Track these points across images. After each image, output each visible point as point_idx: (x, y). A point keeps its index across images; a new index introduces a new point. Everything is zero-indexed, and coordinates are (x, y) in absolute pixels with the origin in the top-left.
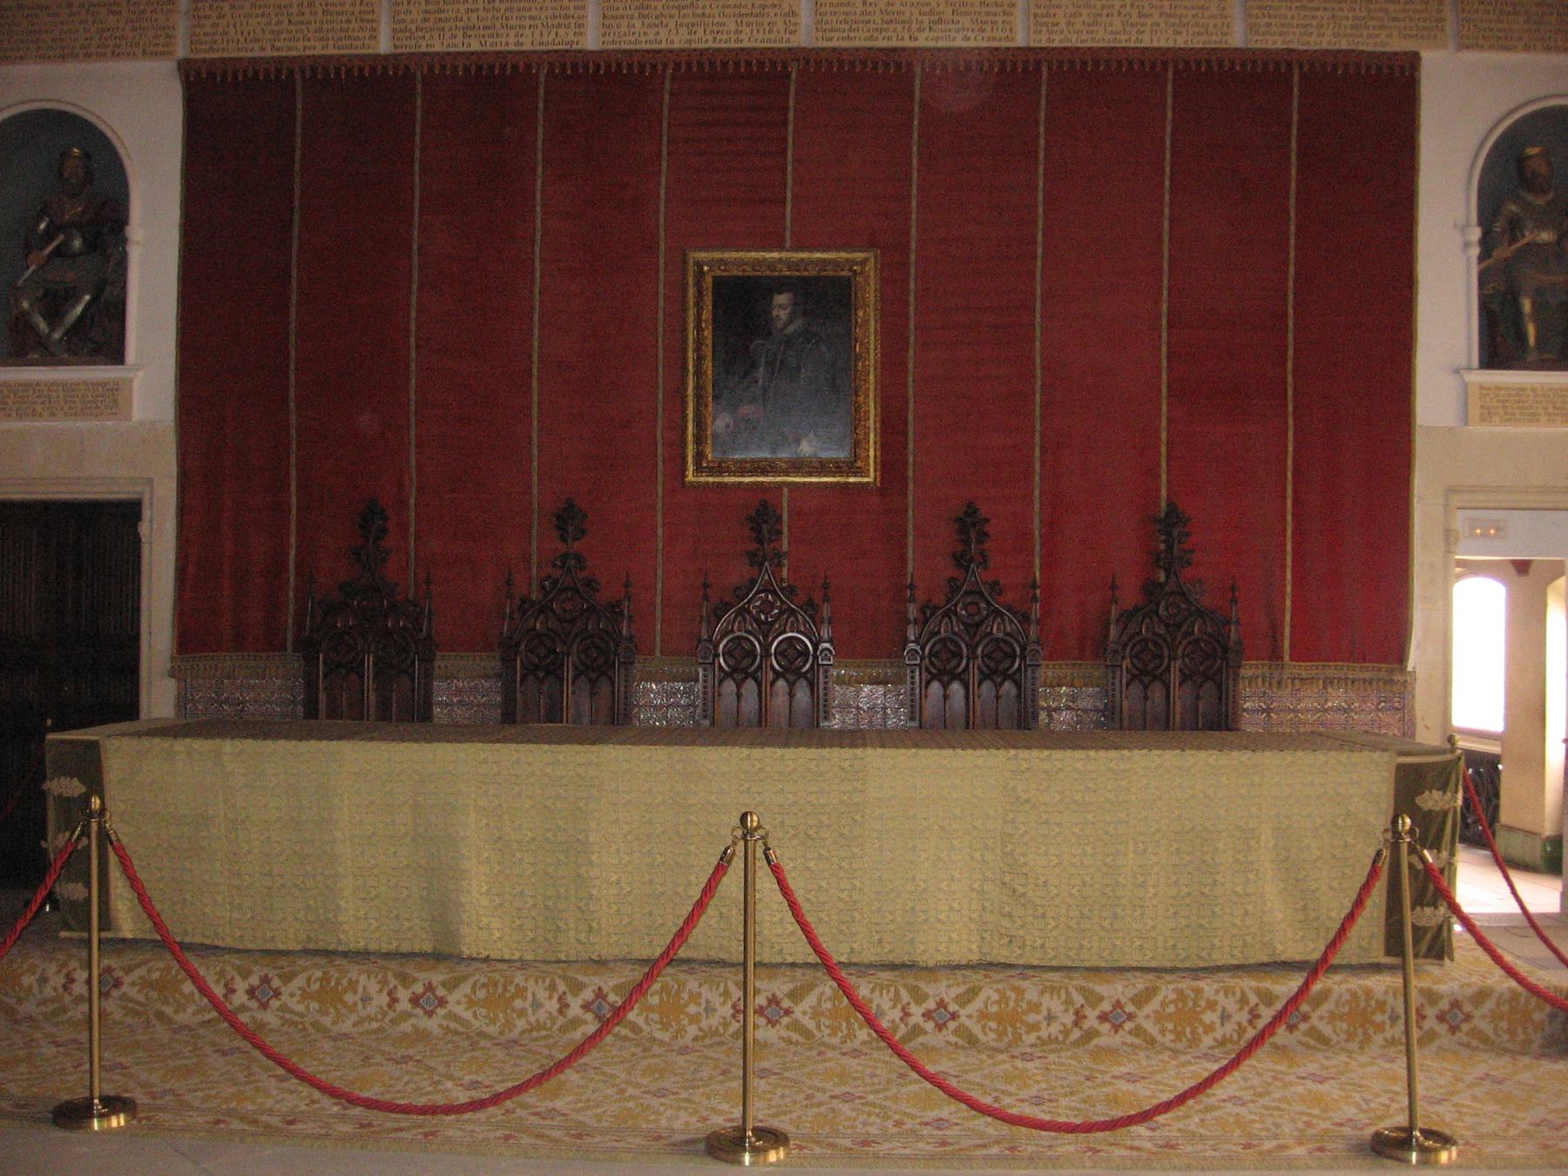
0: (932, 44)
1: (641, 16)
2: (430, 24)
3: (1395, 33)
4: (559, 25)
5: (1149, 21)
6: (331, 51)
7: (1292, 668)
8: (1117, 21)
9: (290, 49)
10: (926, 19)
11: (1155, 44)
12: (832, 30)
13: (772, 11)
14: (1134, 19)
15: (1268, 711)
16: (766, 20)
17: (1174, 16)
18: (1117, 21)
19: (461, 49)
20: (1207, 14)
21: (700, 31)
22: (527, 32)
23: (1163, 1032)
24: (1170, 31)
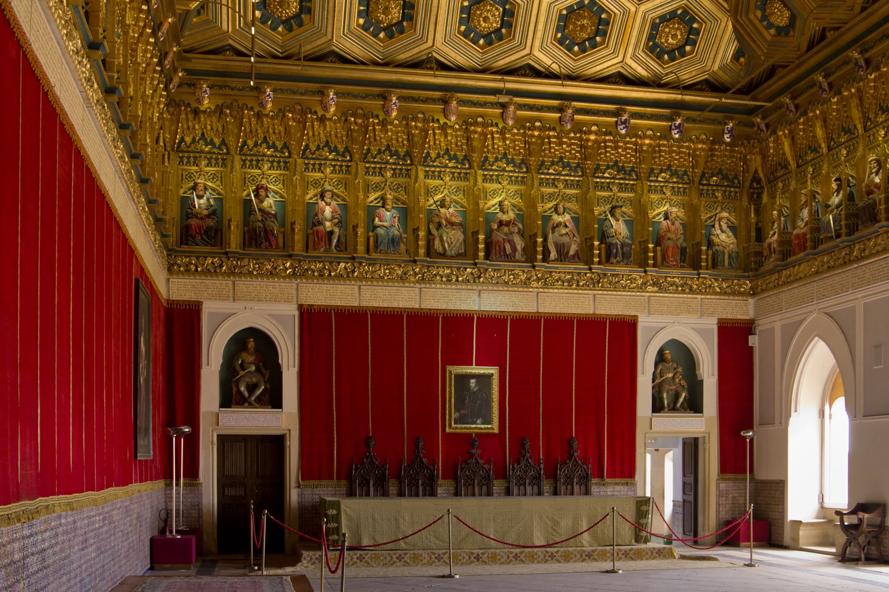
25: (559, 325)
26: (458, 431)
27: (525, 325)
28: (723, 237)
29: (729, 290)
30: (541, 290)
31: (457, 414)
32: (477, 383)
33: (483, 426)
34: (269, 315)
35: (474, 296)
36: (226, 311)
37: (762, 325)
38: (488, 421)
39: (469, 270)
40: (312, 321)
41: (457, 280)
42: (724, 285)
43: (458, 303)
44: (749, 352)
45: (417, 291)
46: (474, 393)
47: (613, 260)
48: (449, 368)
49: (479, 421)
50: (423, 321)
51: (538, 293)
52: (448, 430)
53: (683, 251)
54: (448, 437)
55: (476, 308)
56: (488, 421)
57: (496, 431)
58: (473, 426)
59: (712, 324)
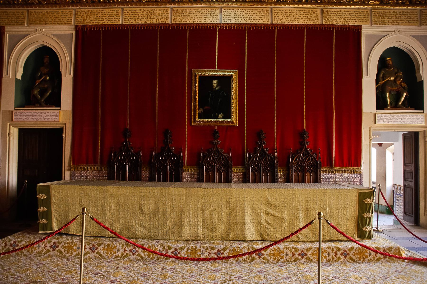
0: (250, 23)
1: (182, 16)
2: (132, 17)
3: (357, 21)
4: (163, 18)
5: (300, 18)
6: (109, 24)
7: (336, 168)
8: (293, 18)
9: (100, 23)
10: (249, 17)
11: (302, 23)
12: (227, 19)
13: (213, 15)
14: (297, 17)
15: (329, 178)
16: (211, 17)
17: (306, 17)
18: (293, 18)
19: (139, 23)
20: (314, 16)
21: (196, 19)
22: (155, 19)
23: (314, 258)
24: (305, 20)
25: (291, 34)
26: (202, 124)
27: (260, 34)
30: (274, 6)
31: (201, 110)
33: (223, 120)
34: (54, 35)
35: (217, 12)
36: (22, 33)
40: (87, 39)
43: (203, 18)
45: (169, 10)
49: (220, 116)
50: (174, 34)
51: (272, 8)
55: (218, 22)
56: (228, 115)
58: (215, 120)
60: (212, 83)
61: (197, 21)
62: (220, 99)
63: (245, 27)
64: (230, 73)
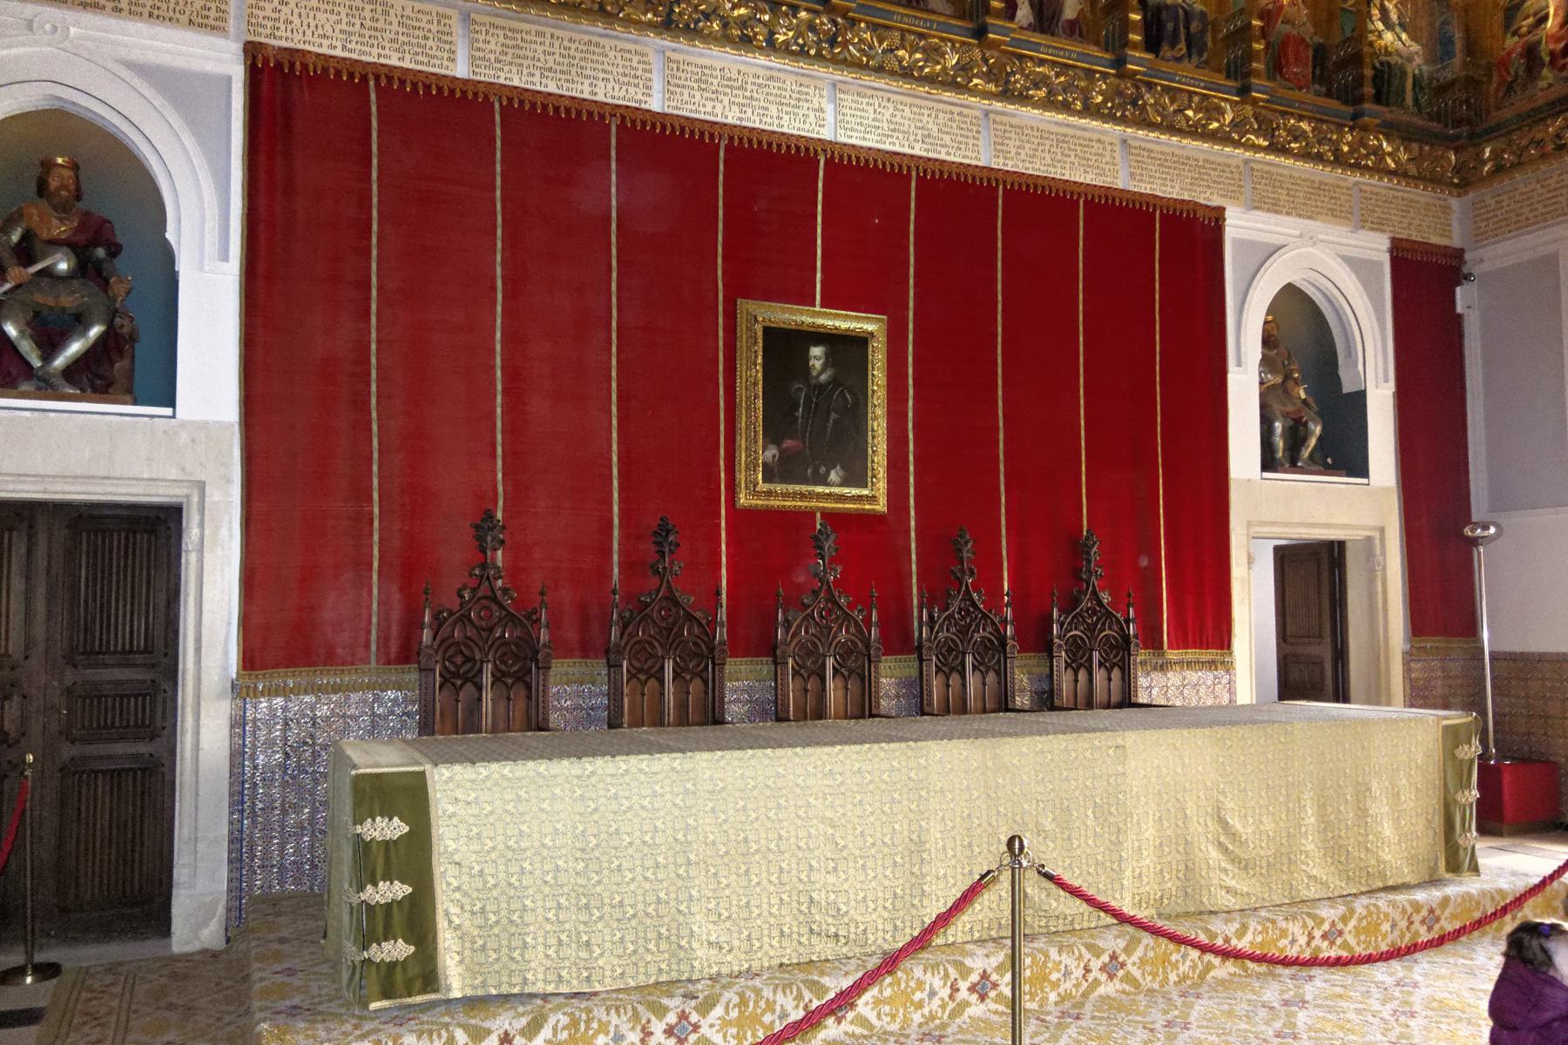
0: (924, 154)
1: (700, 89)
2: (508, 58)
4: (629, 84)
6: (406, 64)
9: (364, 53)
10: (920, 132)
12: (852, 130)
13: (806, 105)
16: (801, 112)
18: (1048, 157)
19: (538, 88)
21: (749, 111)
22: (601, 84)
26: (775, 503)
28: (1388, 37)
29: (1413, 170)
31: (772, 452)
32: (830, 359)
37: (1487, 259)
38: (857, 476)
39: (803, 14)
41: (771, 41)
42: (1404, 157)
43: (773, 110)
44: (1453, 326)
46: (821, 388)
47: (1166, 51)
48: (746, 306)
49: (833, 476)
52: (743, 500)
53: (1320, 53)
54: (740, 517)
56: (857, 476)
57: (881, 506)
58: (819, 489)
59: (1376, 247)
60: (806, 358)
61: (753, 120)
62: (833, 416)
63: (909, 168)
64: (870, 327)
